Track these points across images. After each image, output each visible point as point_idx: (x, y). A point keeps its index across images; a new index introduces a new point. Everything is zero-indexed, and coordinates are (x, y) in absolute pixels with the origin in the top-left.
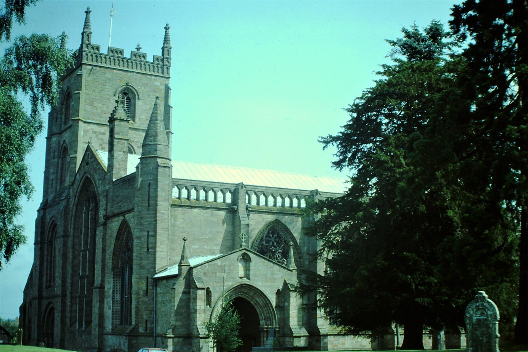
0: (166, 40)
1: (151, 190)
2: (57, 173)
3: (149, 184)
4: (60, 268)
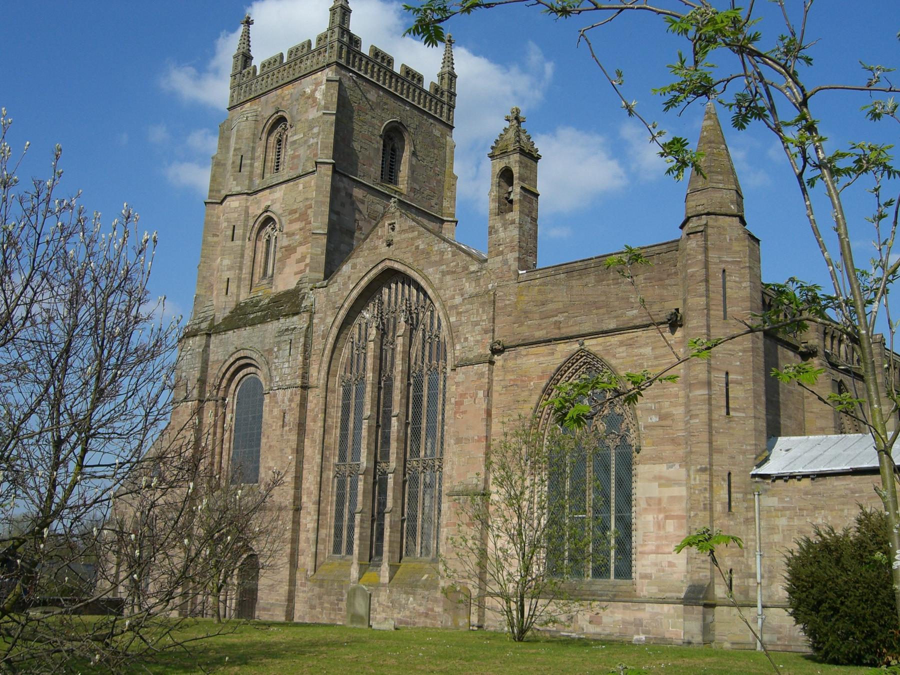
1: (728, 284)
2: (241, 269)
3: (724, 271)
4: (289, 451)
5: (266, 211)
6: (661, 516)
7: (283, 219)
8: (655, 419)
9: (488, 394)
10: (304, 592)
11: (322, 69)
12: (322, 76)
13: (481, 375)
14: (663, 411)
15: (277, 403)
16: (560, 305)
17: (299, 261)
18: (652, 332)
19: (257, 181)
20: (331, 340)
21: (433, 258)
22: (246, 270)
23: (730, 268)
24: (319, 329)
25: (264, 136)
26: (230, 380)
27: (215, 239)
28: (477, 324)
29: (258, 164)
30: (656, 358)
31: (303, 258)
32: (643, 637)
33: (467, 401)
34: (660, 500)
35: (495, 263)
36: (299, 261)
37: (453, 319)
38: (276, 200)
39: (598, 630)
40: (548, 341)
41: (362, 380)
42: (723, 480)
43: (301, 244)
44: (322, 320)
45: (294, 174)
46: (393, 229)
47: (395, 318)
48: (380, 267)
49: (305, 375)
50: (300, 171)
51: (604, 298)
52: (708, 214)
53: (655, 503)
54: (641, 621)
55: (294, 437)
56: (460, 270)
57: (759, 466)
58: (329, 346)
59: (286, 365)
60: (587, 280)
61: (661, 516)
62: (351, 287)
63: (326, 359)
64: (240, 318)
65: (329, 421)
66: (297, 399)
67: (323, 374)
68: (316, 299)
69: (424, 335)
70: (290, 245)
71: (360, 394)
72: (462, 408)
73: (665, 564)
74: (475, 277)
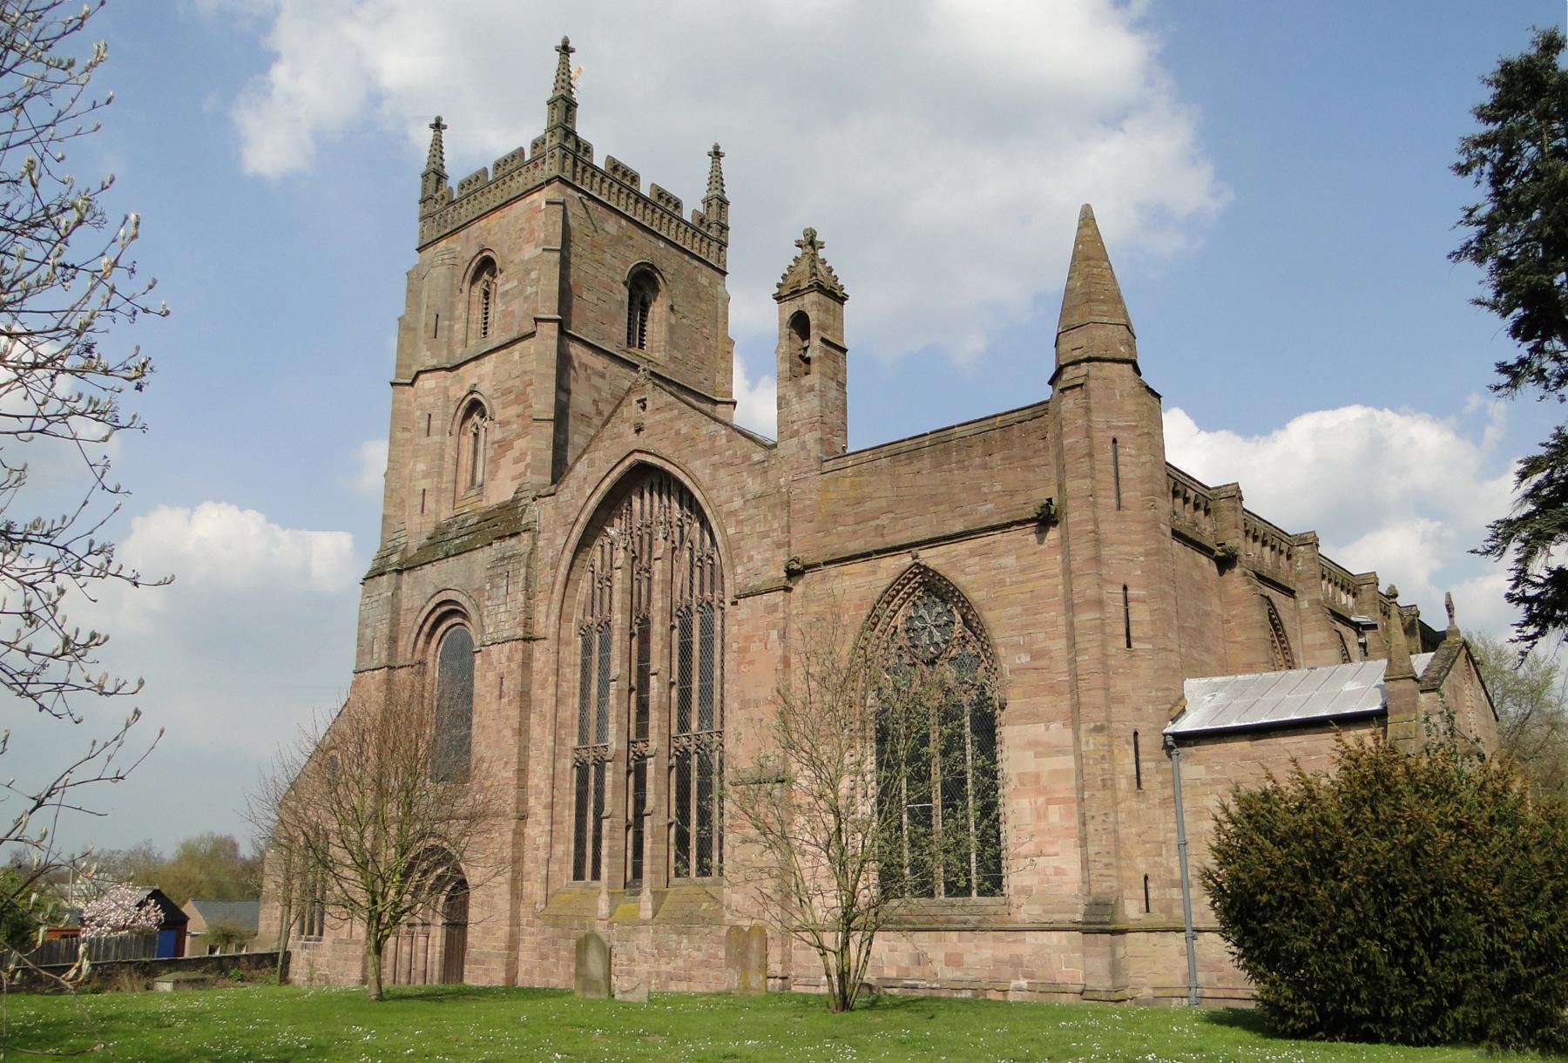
0: (717, 179)
1: (1121, 459)
2: (440, 475)
3: (1115, 441)
5: (471, 392)
6: (1041, 800)
7: (494, 402)
8: (1025, 659)
9: (783, 636)
10: (532, 934)
11: (539, 188)
12: (539, 198)
13: (773, 608)
14: (1035, 647)
15: (491, 664)
16: (883, 503)
17: (516, 461)
18: (1015, 534)
19: (459, 350)
20: (563, 570)
21: (700, 446)
22: (447, 477)
23: (1122, 436)
24: (546, 554)
25: (466, 287)
26: (430, 635)
27: (407, 435)
28: (765, 535)
29: (459, 327)
30: (1022, 571)
31: (523, 455)
32: (1024, 983)
33: (756, 646)
34: (1038, 776)
35: (789, 448)
36: (516, 461)
37: (731, 531)
38: (483, 376)
39: (958, 974)
40: (866, 556)
41: (607, 624)
42: (1128, 743)
43: (519, 436)
44: (550, 541)
45: (506, 338)
46: (644, 408)
47: (650, 535)
48: (627, 463)
49: (528, 622)
50: (515, 334)
51: (944, 489)
52: (1089, 360)
53: (1032, 782)
54: (1019, 957)
55: (514, 713)
56: (738, 461)
57: (1174, 720)
58: (561, 579)
59: (503, 609)
60: (917, 465)
61: (1041, 800)
62: (588, 492)
63: (557, 597)
64: (439, 545)
65: (565, 686)
66: (518, 656)
67: (553, 618)
68: (540, 513)
69: (692, 556)
70: (504, 439)
71: (605, 646)
72: (749, 657)
73: (1050, 871)
74: (762, 469)
